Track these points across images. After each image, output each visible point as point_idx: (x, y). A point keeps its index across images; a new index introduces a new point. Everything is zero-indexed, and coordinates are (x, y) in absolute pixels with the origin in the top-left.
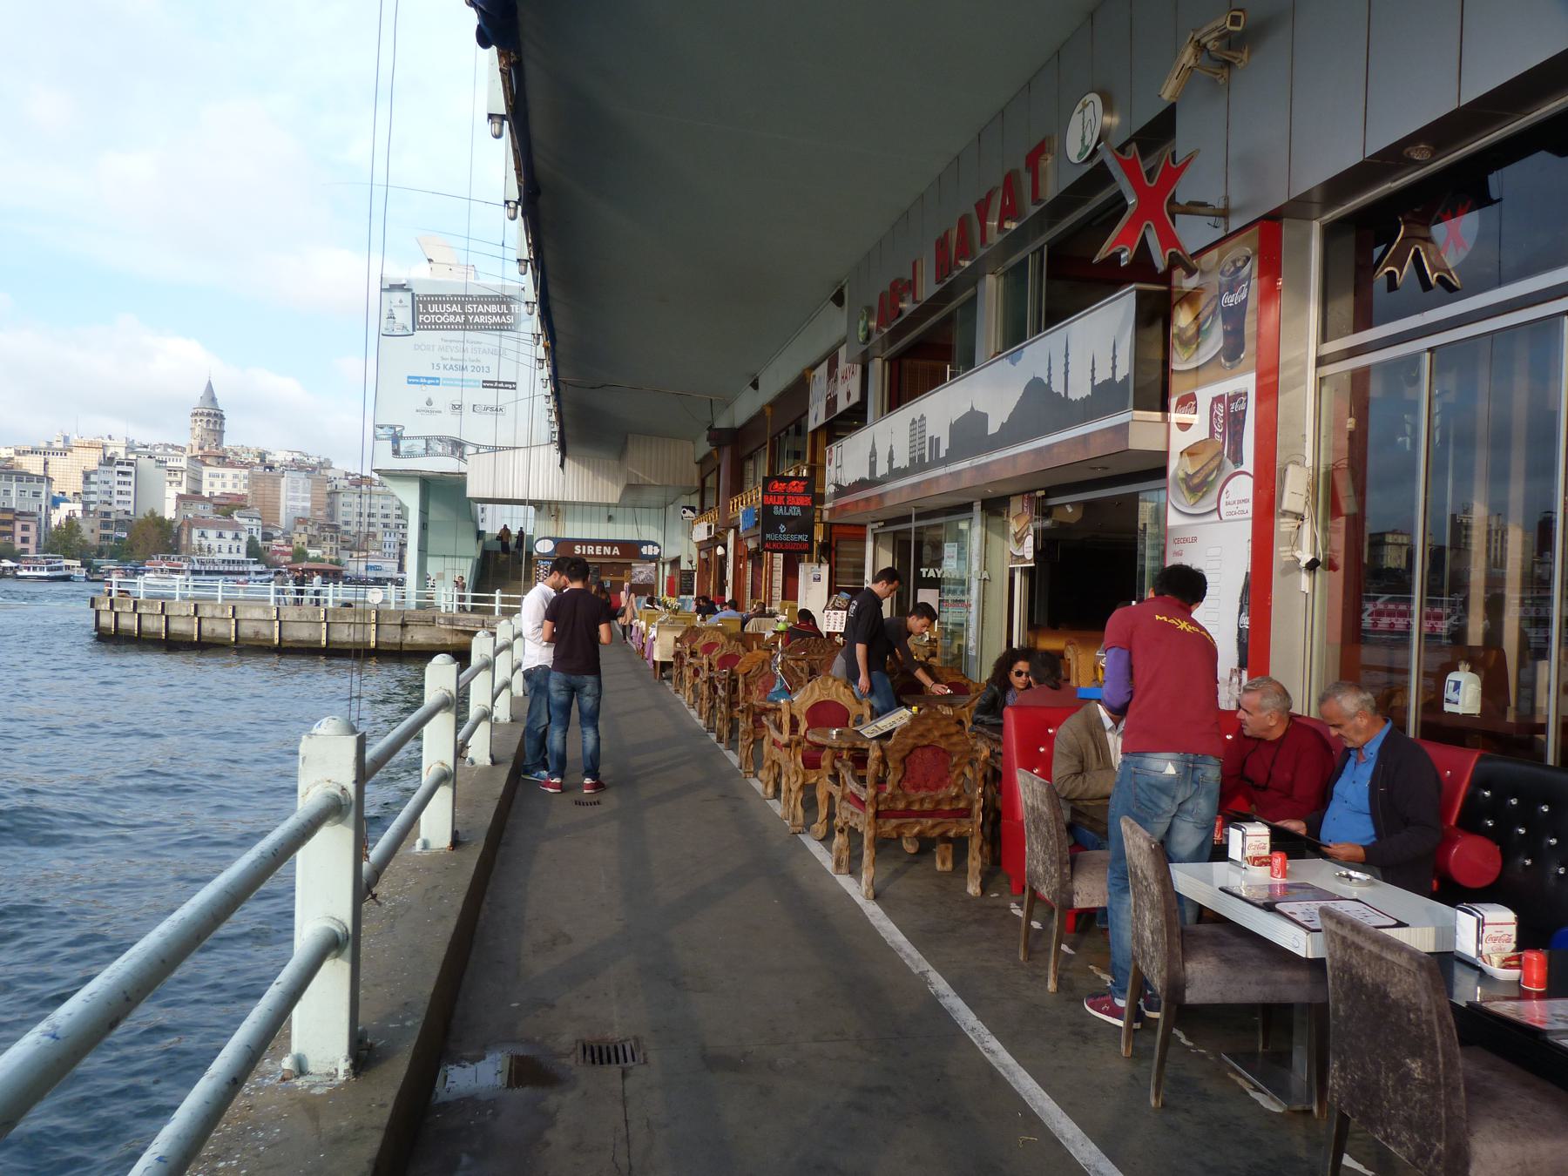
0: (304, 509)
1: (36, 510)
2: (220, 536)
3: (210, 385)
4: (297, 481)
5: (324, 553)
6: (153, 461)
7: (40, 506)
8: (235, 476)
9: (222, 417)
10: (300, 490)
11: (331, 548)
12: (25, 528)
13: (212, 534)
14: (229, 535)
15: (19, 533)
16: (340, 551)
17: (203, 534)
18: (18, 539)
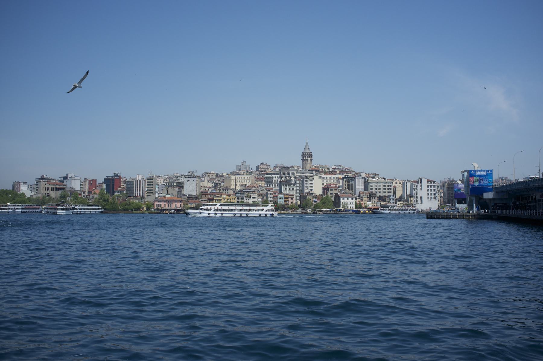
0: (362, 189)
1: (293, 194)
2: (348, 199)
3: (307, 144)
4: (359, 180)
5: (372, 203)
6: (318, 176)
7: (294, 192)
8: (330, 178)
9: (312, 155)
10: (360, 182)
11: (374, 201)
12: (292, 199)
13: (346, 199)
14: (350, 199)
15: (290, 201)
16: (377, 202)
17: (343, 199)
18: (290, 203)
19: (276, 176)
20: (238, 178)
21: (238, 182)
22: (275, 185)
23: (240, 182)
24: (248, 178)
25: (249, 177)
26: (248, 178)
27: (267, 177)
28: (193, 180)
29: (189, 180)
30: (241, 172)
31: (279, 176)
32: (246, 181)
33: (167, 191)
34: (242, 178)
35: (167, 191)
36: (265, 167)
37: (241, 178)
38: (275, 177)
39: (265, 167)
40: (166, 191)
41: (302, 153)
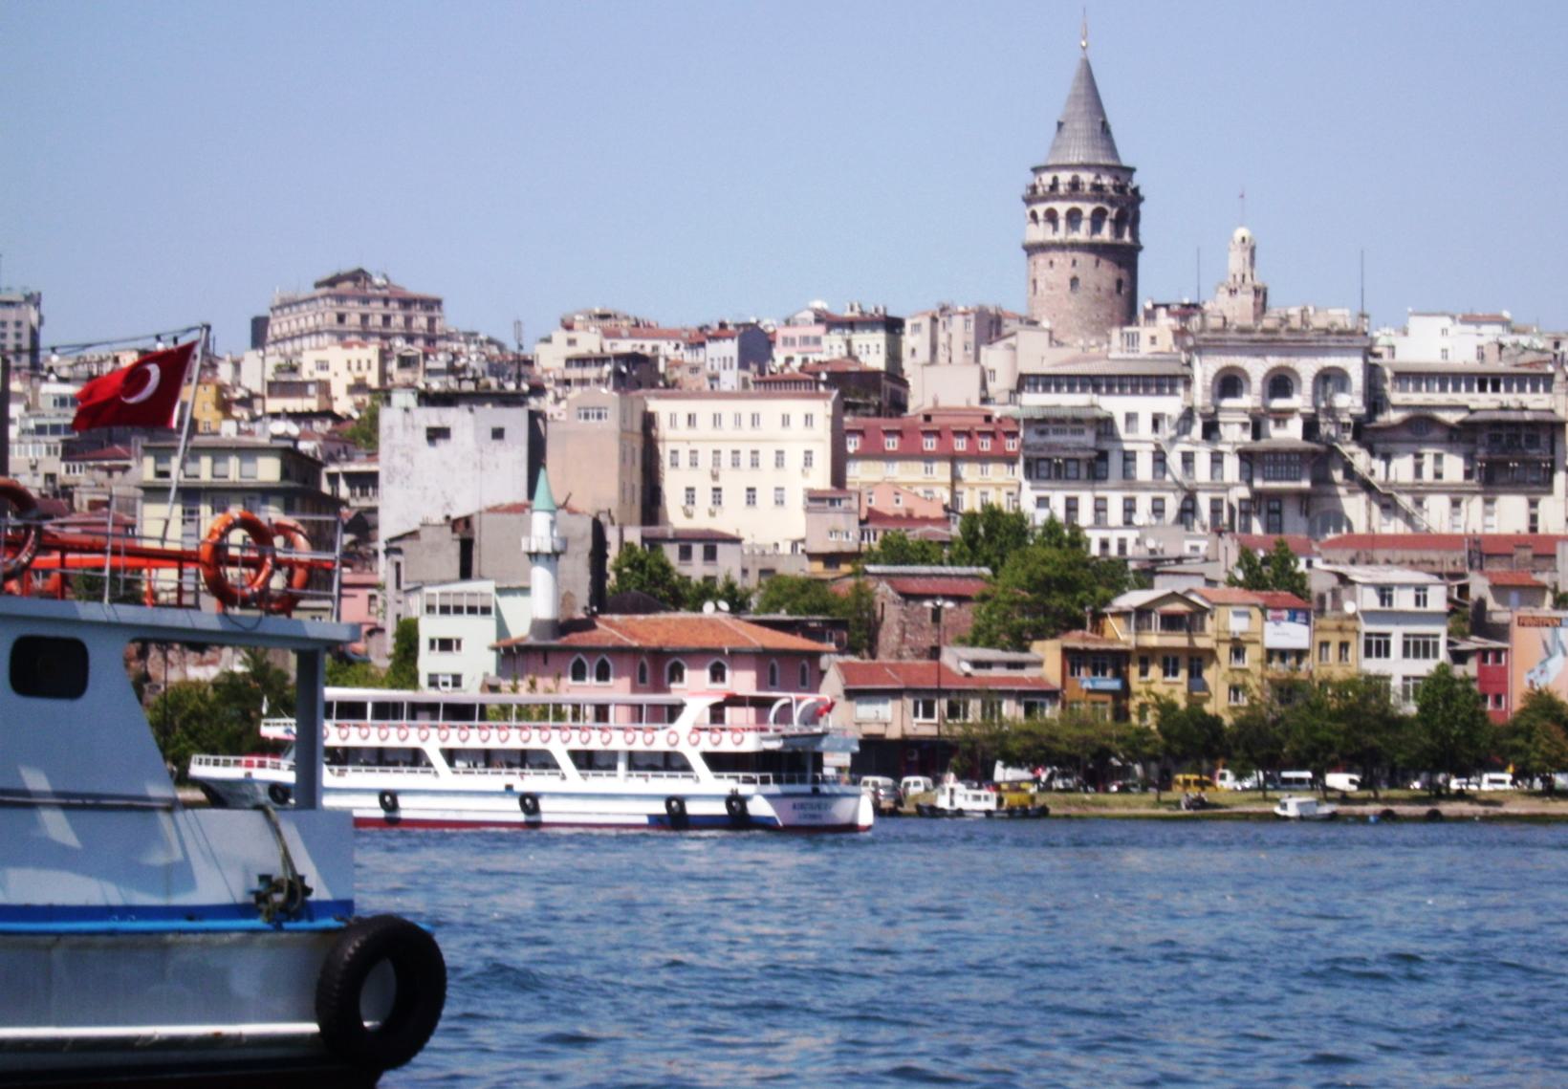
19: (1145, 405)
20: (682, 420)
21: (675, 464)
22: (1129, 508)
23: (705, 460)
24: (797, 420)
25: (808, 419)
26: (797, 420)
27: (1044, 421)
28: (498, 434)
29: (436, 434)
30: (323, 366)
31: (1171, 405)
32: (767, 459)
33: (467, 547)
34: (727, 421)
35: (467, 547)
36: (386, 319)
37: (717, 419)
38: (1131, 418)
39: (386, 319)
40: (454, 550)
41: (1031, 179)
